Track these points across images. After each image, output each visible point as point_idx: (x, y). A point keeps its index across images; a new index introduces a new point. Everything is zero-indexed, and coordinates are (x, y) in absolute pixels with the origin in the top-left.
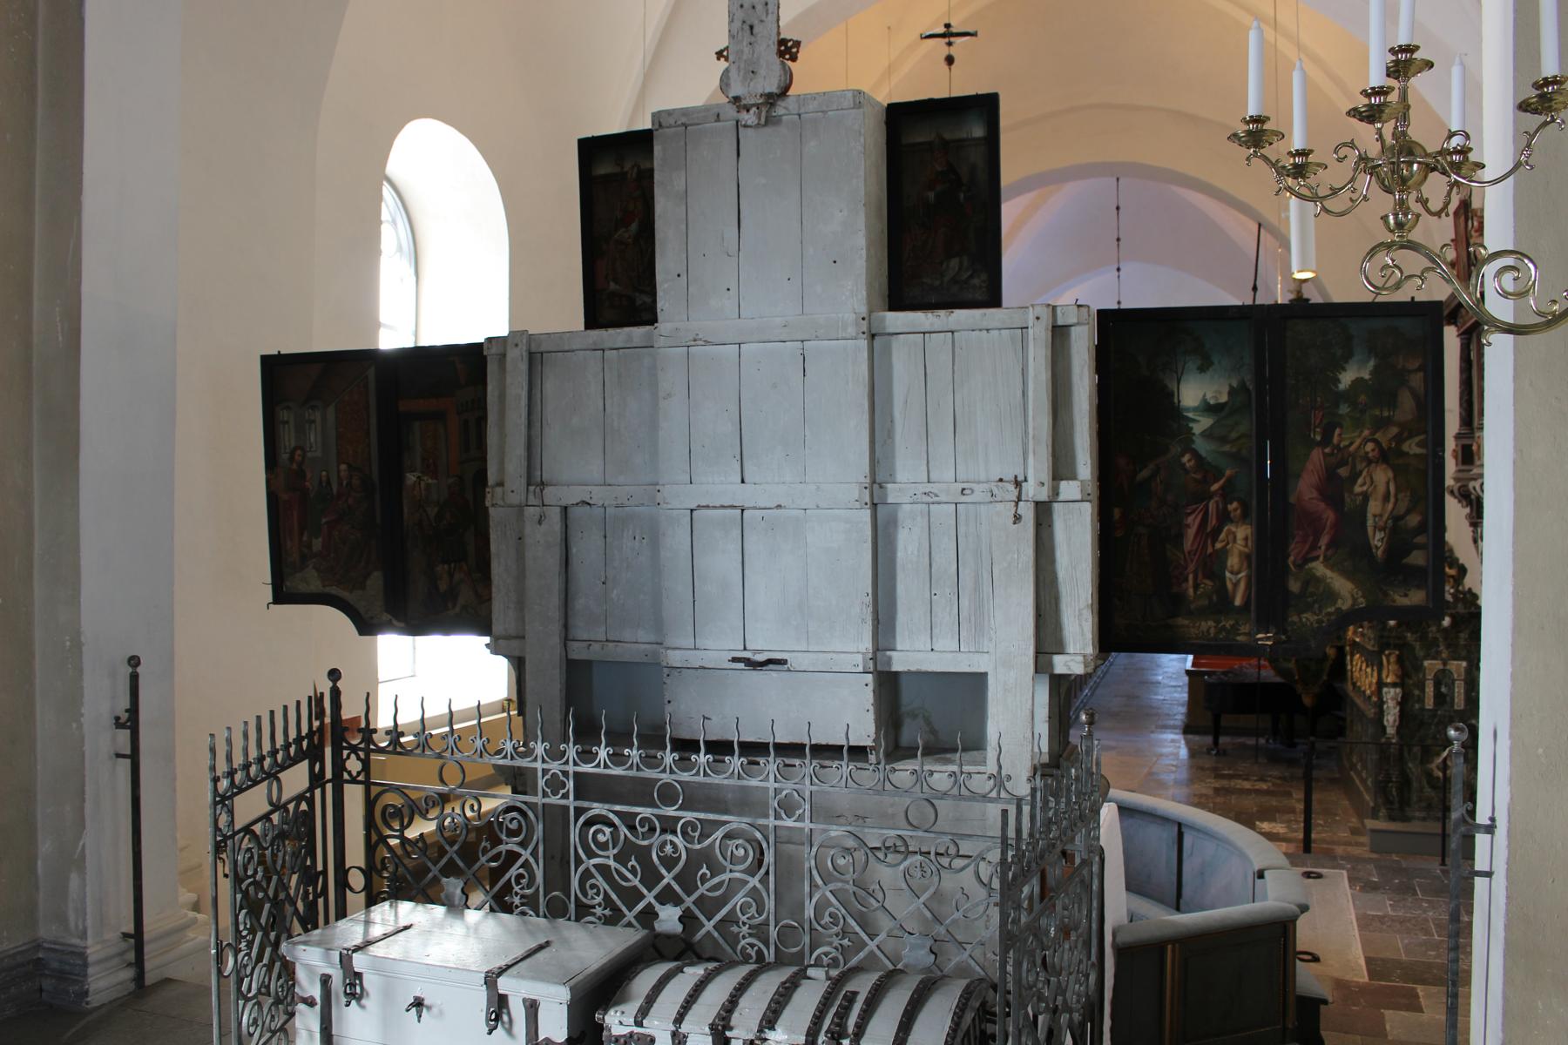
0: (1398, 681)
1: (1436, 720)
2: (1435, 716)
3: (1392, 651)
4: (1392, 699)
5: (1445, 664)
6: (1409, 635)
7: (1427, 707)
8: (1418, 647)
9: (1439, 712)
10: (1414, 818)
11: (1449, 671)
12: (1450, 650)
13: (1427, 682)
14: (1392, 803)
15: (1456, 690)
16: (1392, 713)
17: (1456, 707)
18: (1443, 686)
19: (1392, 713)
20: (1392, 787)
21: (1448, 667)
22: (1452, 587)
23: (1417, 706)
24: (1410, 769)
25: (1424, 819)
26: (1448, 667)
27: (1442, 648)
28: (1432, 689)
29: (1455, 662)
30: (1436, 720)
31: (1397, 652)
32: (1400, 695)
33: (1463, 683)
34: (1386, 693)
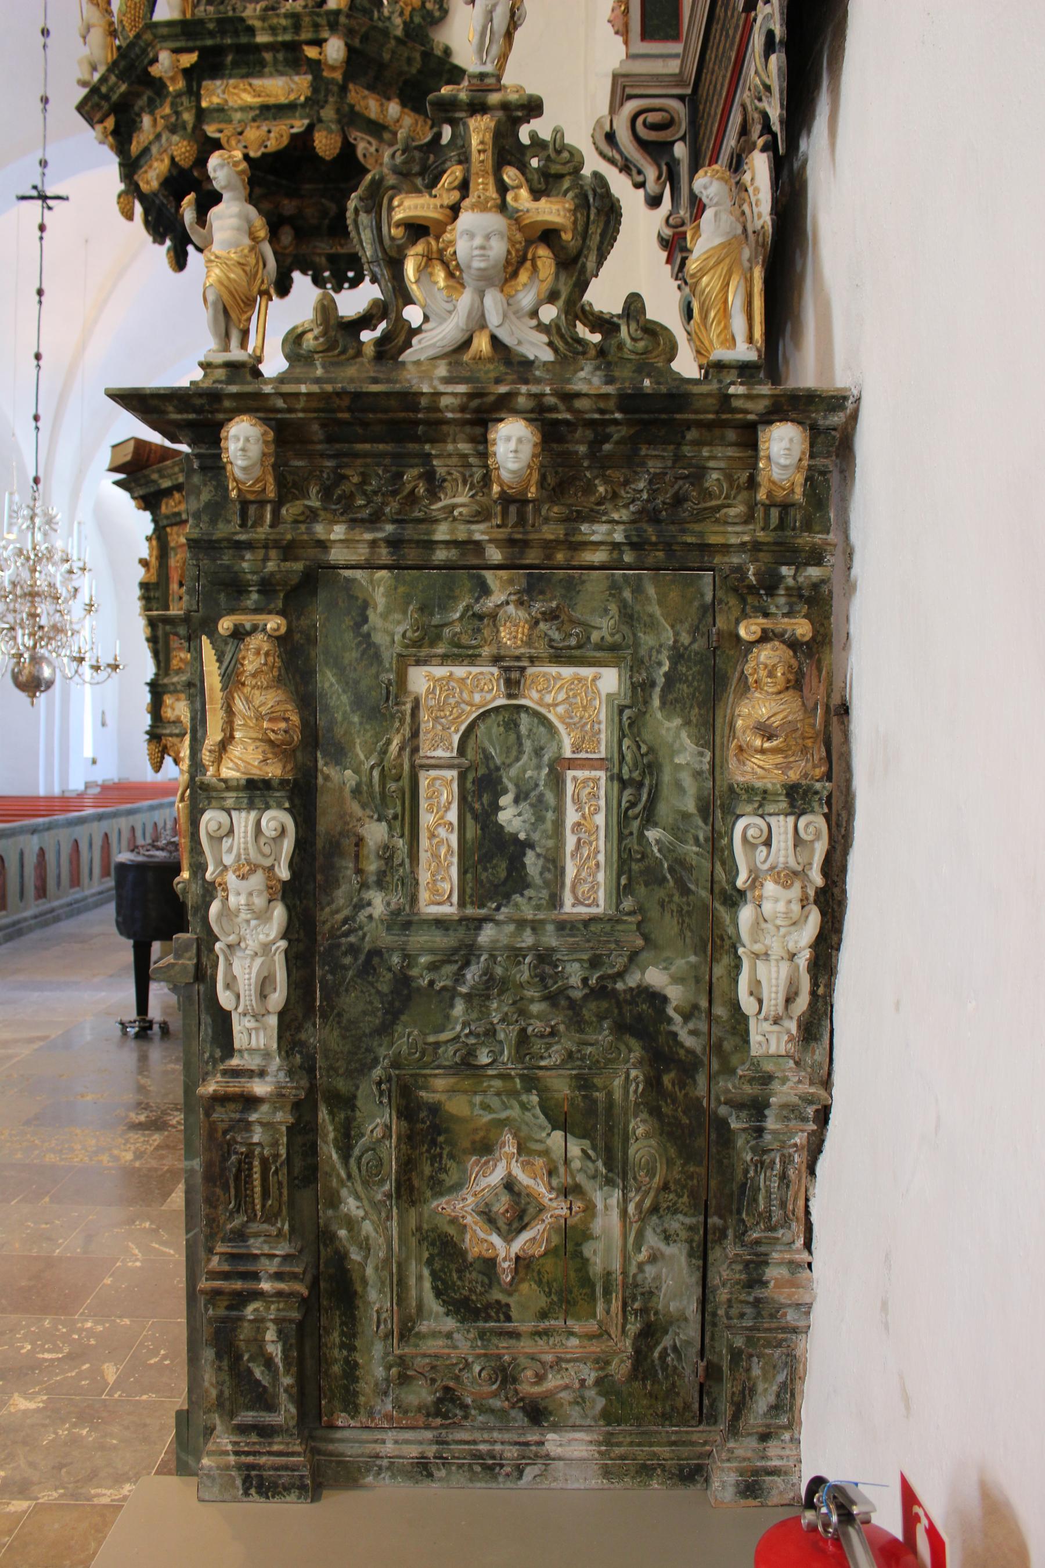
0: (274, 771)
1: (472, 974)
2: (466, 953)
3: (247, 620)
4: (247, 869)
5: (513, 685)
6: (339, 531)
7: (429, 908)
8: (380, 598)
9: (487, 935)
10: (372, 1464)
11: (544, 721)
12: (538, 607)
13: (425, 779)
14: (264, 1400)
15: (572, 816)
16: (252, 943)
17: (569, 907)
18: (505, 800)
19: (252, 943)
20: (259, 1322)
21: (529, 699)
22: (552, 297)
23: (379, 904)
24: (351, 1223)
25: (423, 1469)
26: (529, 699)
27: (498, 597)
28: (453, 816)
29: (567, 672)
30: (472, 974)
31: (274, 623)
32: (288, 845)
33: (602, 774)
34: (216, 840)
